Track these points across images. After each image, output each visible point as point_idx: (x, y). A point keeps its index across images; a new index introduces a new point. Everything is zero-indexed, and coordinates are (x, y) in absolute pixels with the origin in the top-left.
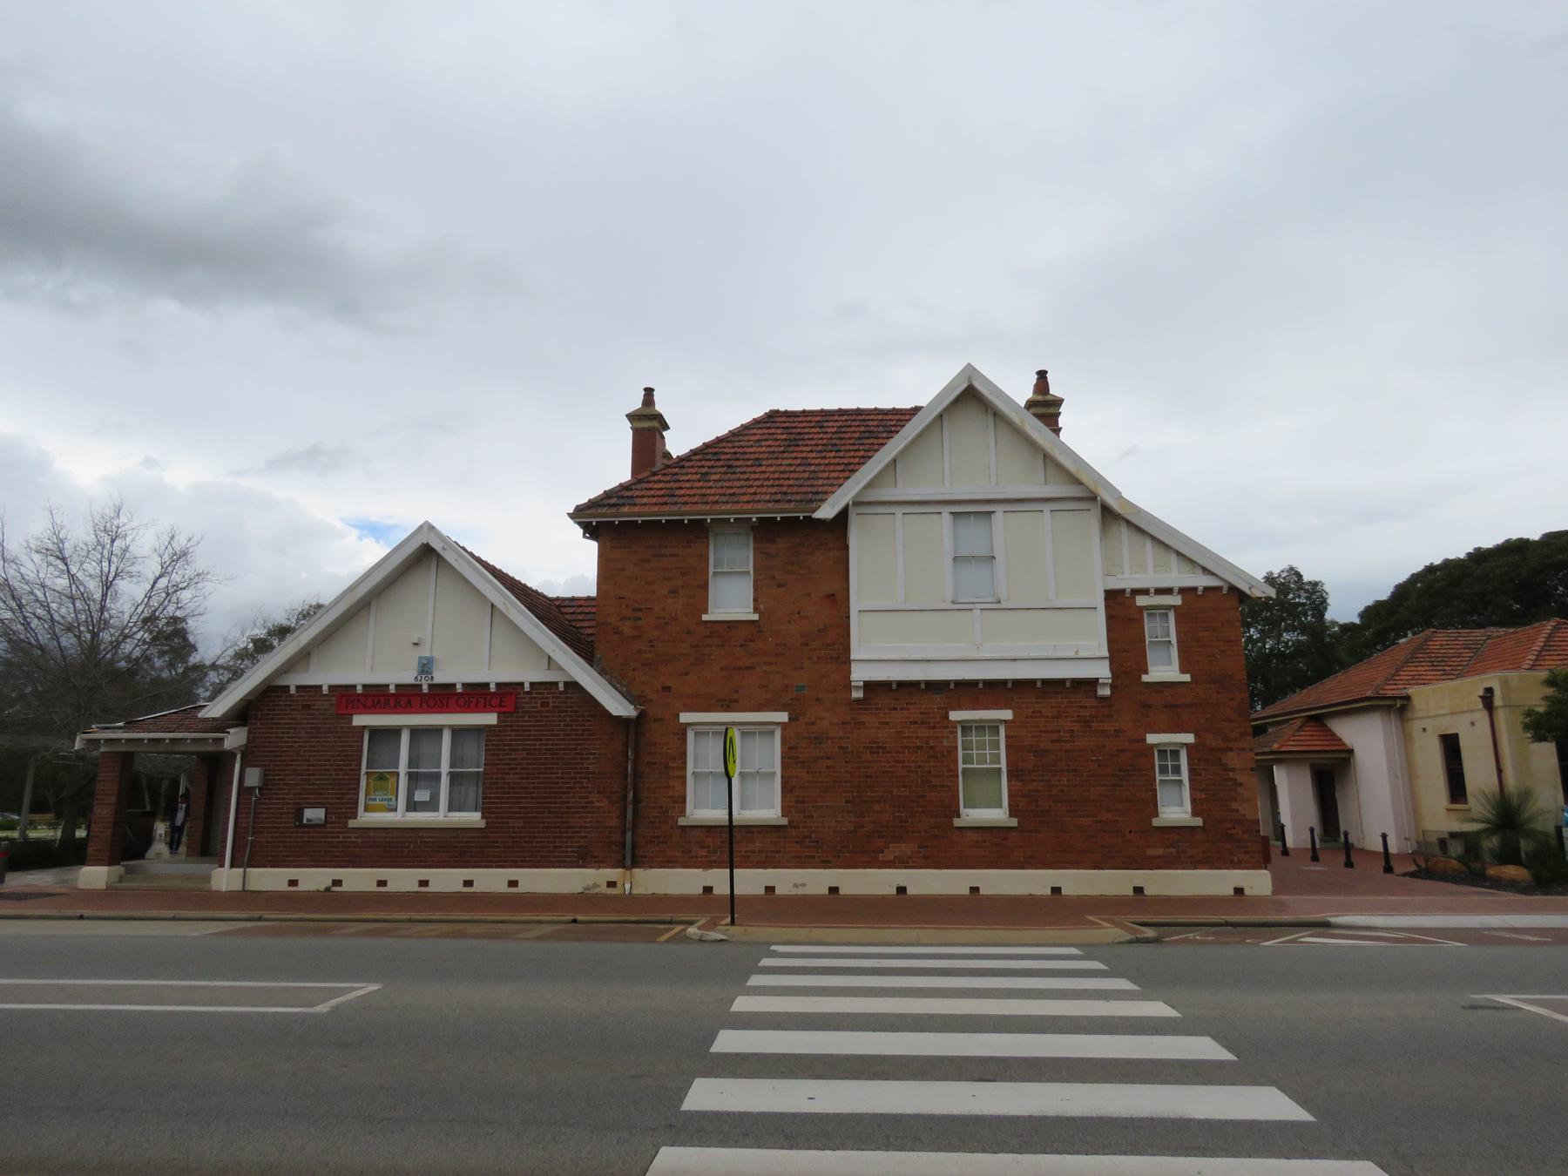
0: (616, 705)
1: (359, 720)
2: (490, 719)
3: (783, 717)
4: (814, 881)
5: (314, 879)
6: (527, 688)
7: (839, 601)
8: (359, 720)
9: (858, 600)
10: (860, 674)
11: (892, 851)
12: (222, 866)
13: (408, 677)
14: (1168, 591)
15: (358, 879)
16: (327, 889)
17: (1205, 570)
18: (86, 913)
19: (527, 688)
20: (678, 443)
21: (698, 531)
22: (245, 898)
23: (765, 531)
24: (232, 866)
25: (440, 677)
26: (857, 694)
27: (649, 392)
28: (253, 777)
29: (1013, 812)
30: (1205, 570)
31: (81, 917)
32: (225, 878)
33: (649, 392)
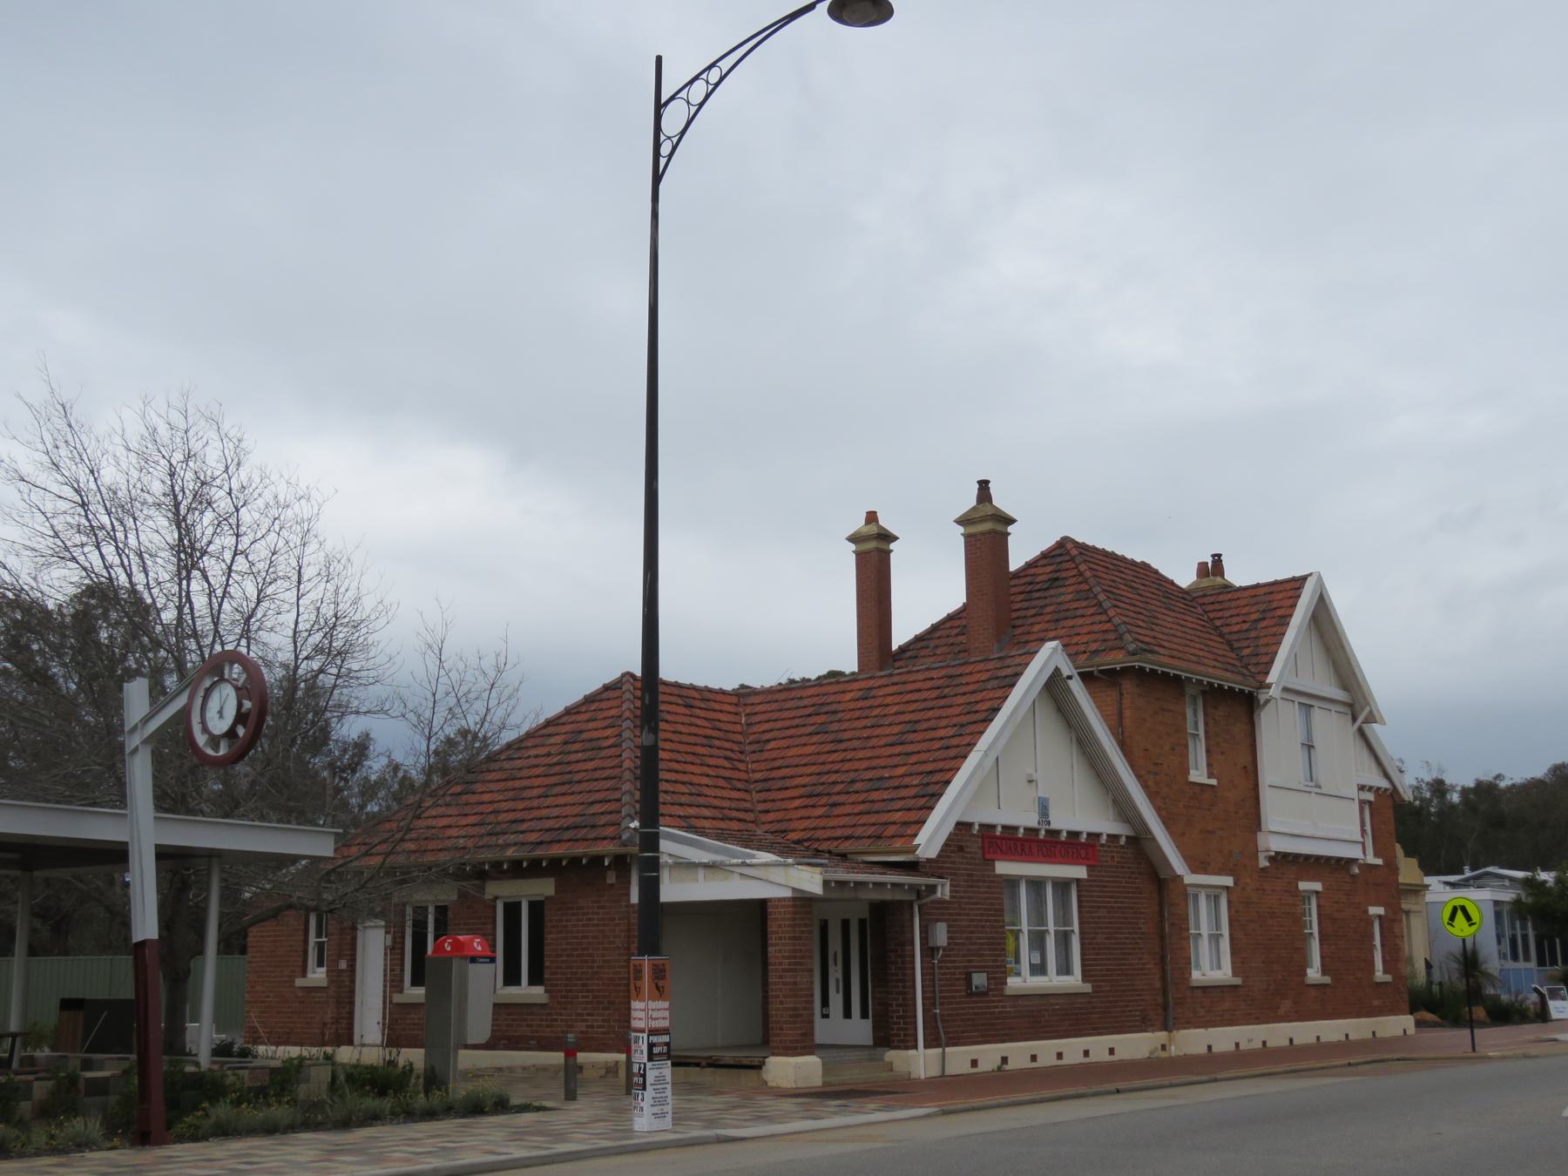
0: (1178, 865)
1: (1004, 868)
2: (1080, 872)
3: (1228, 881)
4: (1135, 1045)
5: (989, 1055)
6: (1103, 840)
7: (1251, 771)
8: (1004, 868)
9: (1269, 773)
10: (1272, 843)
11: (1286, 1005)
12: (916, 1047)
13: (1031, 820)
14: (1370, 788)
15: (1018, 1053)
16: (999, 1068)
17: (1387, 776)
18: (1121, 1086)
19: (1103, 840)
20: (1021, 551)
21: (1174, 684)
22: (945, 1087)
23: (1214, 695)
24: (926, 1047)
25: (1054, 826)
26: (1263, 863)
27: (984, 485)
28: (941, 934)
29: (1086, 976)
30: (1387, 776)
31: (1118, 1091)
32: (920, 1061)
33: (984, 485)
